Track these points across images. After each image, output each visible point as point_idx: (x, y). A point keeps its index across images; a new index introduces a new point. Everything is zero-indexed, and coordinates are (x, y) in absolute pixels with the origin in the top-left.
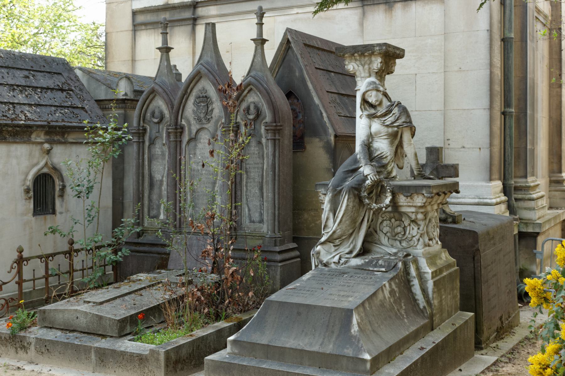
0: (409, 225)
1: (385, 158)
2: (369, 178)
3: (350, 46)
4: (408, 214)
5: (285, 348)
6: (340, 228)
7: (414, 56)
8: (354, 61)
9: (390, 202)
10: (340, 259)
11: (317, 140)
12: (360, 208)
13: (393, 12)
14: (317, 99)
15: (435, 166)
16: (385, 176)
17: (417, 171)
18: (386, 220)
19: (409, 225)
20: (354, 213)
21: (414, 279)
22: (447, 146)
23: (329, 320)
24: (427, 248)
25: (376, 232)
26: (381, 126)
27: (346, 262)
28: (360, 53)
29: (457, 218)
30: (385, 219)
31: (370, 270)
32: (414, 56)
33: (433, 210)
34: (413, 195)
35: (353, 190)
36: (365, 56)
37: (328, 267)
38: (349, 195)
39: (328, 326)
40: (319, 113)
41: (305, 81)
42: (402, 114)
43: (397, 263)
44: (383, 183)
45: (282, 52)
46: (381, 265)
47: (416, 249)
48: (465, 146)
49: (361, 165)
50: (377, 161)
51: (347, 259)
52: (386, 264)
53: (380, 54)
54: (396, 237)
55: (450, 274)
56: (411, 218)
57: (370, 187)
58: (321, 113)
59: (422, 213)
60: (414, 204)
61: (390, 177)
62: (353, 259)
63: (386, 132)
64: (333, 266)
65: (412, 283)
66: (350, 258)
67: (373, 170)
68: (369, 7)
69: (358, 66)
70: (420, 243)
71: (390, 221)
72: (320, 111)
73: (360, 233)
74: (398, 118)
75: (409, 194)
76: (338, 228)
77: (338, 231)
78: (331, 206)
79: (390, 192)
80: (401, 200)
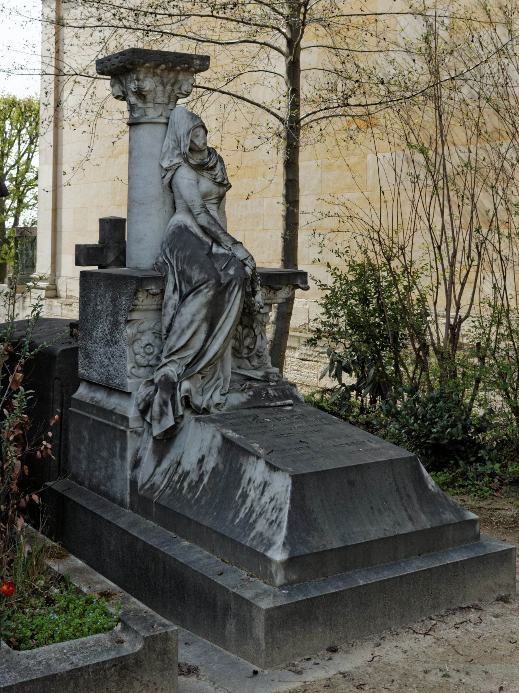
5: (372, 541)
23: (395, 481)
39: (398, 490)
46: (275, 396)
78: (208, 312)
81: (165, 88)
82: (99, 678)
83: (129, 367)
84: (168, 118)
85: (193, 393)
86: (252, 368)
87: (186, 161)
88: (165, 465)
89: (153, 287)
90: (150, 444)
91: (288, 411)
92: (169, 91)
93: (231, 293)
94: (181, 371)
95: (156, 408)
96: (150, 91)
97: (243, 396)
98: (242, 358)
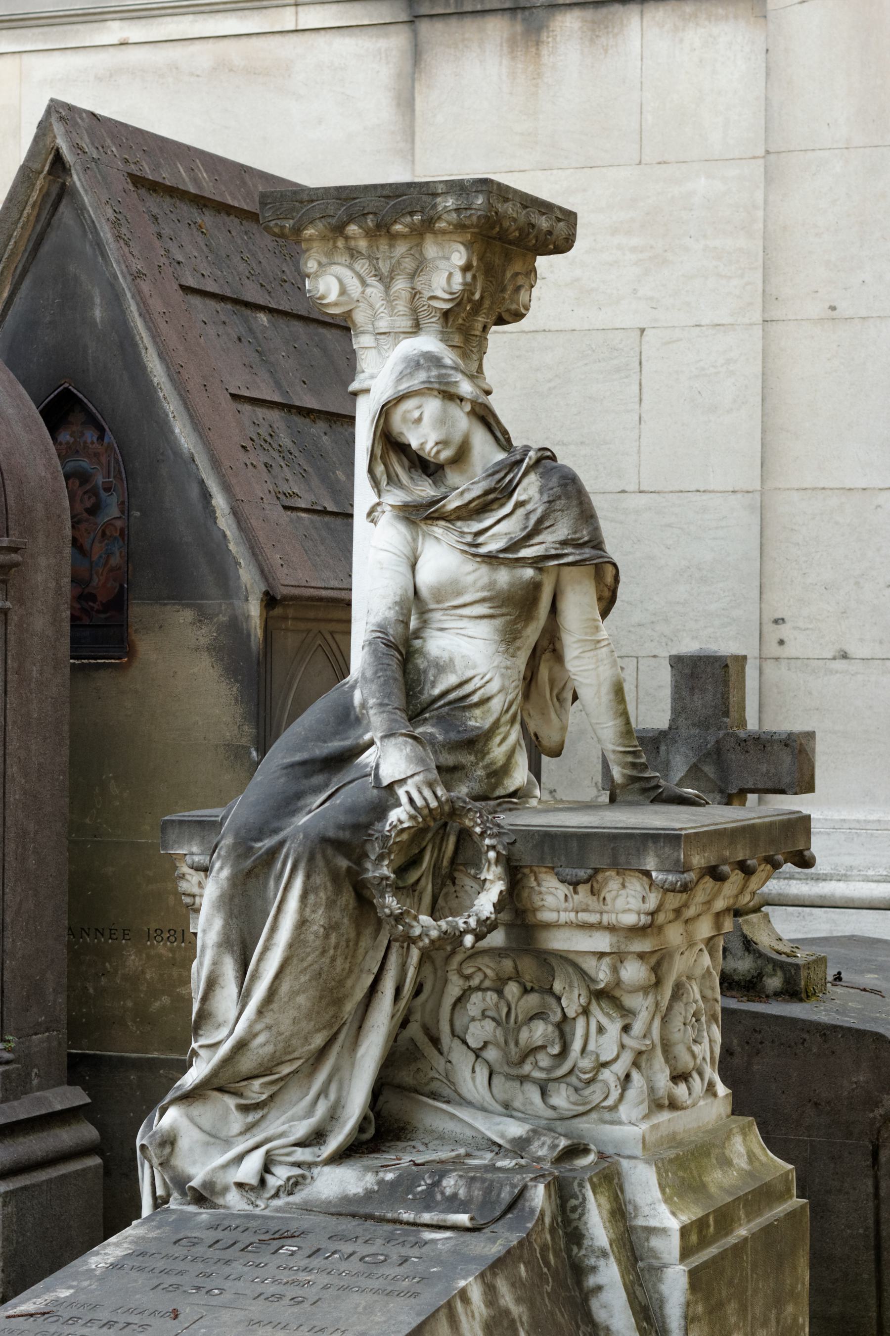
0: (586, 1012)
1: (477, 705)
2: (404, 799)
3: (327, 189)
4: (580, 961)
6: (269, 1028)
7: (634, 250)
8: (344, 259)
9: (499, 907)
10: (266, 1168)
11: (187, 615)
12: (359, 934)
13: (544, 51)
14: (189, 428)
15: (712, 740)
16: (477, 788)
17: (624, 765)
18: (479, 988)
19: (586, 1012)
20: (333, 960)
21: (602, 1263)
22: (772, 649)
24: (665, 1116)
25: (435, 1041)
26: (458, 554)
27: (294, 1185)
28: (370, 222)
29: (803, 973)
30: (475, 982)
31: (401, 1222)
32: (634, 250)
33: (691, 945)
34: (600, 877)
35: (330, 852)
36: (393, 237)
37: (214, 1206)
38: (308, 876)
40: (194, 492)
41: (135, 345)
42: (559, 504)
43: (524, 1188)
44: (468, 823)
45: (28, 210)
46: (455, 1195)
47: (612, 1123)
48: (853, 649)
49: (367, 737)
50: (440, 721)
51: (297, 1171)
52: (477, 1193)
53: (461, 227)
54: (527, 1068)
55: (767, 1230)
56: (594, 981)
57: (405, 837)
58: (206, 496)
59: (641, 956)
60: (606, 919)
61: (500, 792)
62: (327, 1169)
63: (483, 589)
64: (234, 1200)
65: (592, 1281)
66: (314, 1164)
67: (421, 761)
68: (439, 26)
69: (364, 283)
70: (631, 1093)
71: (500, 992)
72: (202, 482)
73: (361, 1051)
74: (540, 521)
75: (582, 874)
76: (259, 1027)
77: (260, 1039)
78: (227, 925)
79: (497, 861)
80: (550, 901)
81: (387, 288)
89: (195, 849)
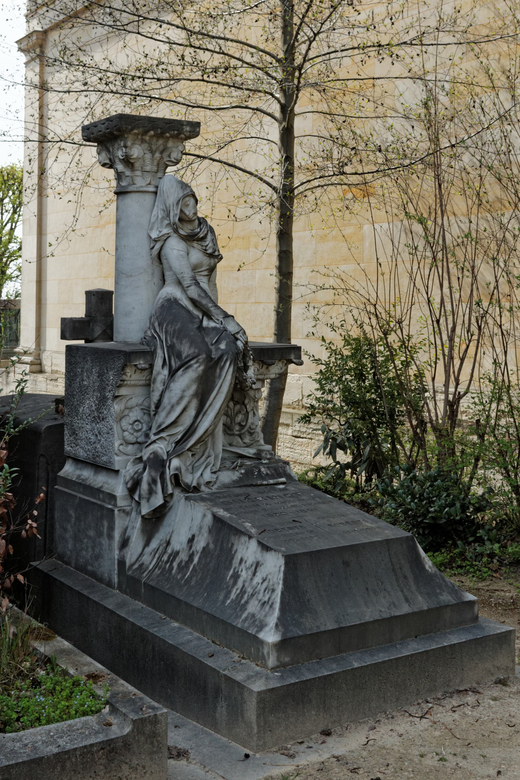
5: (367, 623)
23: (391, 562)
39: (394, 570)
46: (267, 474)
78: (198, 387)
81: (153, 155)
82: (87, 762)
83: (116, 444)
84: (157, 187)
85: (183, 471)
86: (245, 445)
87: (176, 231)
88: (154, 544)
89: (141, 362)
90: (139, 523)
91: (281, 490)
92: (158, 158)
93: (222, 368)
94: (170, 448)
95: (144, 486)
96: (138, 158)
97: (234, 474)
98: (233, 435)
